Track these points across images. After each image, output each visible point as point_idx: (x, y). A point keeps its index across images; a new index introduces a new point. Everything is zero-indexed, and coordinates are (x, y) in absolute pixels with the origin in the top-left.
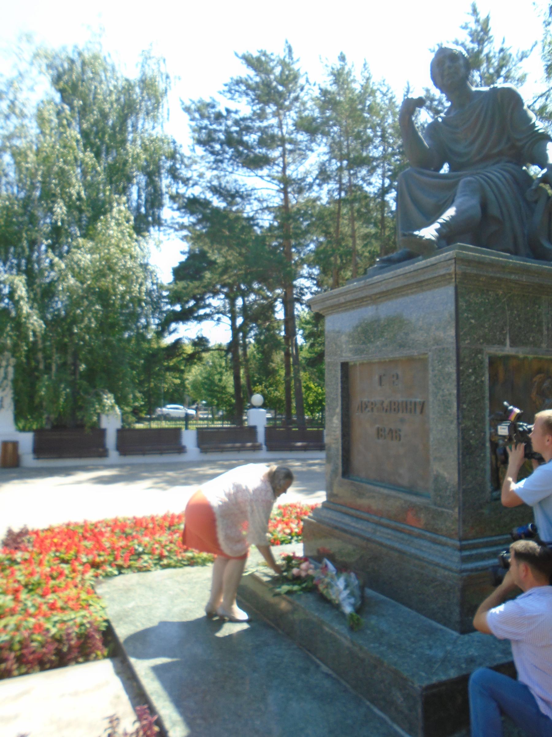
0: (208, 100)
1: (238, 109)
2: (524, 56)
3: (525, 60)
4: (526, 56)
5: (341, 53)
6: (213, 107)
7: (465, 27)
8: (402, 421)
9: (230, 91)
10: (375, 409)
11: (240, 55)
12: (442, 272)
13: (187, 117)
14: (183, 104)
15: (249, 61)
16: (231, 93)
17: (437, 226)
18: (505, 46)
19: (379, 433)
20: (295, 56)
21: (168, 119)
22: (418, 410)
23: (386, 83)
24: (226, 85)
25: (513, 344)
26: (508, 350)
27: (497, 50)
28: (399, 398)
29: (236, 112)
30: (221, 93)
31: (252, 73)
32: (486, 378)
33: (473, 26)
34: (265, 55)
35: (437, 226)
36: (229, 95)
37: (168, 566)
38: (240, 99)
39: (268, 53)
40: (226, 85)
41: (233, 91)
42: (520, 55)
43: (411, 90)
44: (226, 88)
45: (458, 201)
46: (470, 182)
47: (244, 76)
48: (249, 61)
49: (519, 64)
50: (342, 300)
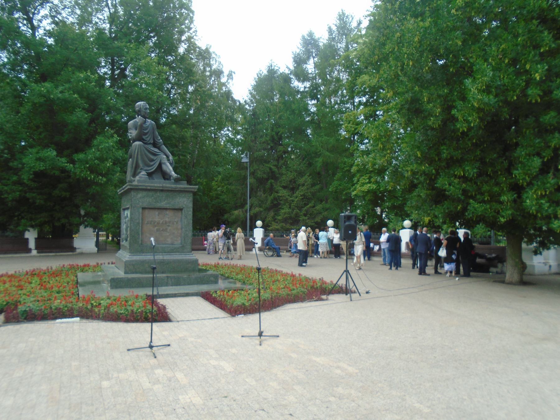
8: (169, 226)
10: (156, 223)
22: (175, 223)
28: (167, 219)
50: (149, 188)
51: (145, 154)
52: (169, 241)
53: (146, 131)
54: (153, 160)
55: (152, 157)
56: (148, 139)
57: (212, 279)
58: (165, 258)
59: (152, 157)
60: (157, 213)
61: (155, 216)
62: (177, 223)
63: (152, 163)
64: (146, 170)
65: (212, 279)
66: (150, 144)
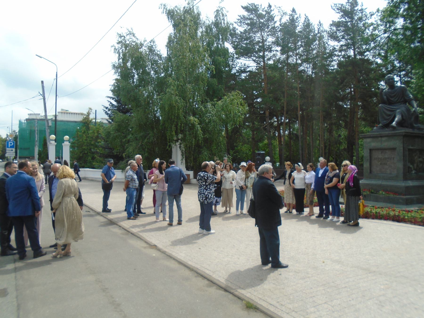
9: (241, 22)
19: (381, 164)
22: (392, 159)
28: (386, 156)
46: (399, 112)
51: (384, 112)
52: (388, 171)
53: (393, 95)
54: (390, 115)
55: (389, 113)
56: (396, 99)
57: (401, 201)
58: (383, 183)
59: (389, 113)
60: (380, 152)
61: (378, 155)
62: (393, 159)
63: (388, 118)
64: (383, 123)
65: (401, 201)
66: (399, 102)
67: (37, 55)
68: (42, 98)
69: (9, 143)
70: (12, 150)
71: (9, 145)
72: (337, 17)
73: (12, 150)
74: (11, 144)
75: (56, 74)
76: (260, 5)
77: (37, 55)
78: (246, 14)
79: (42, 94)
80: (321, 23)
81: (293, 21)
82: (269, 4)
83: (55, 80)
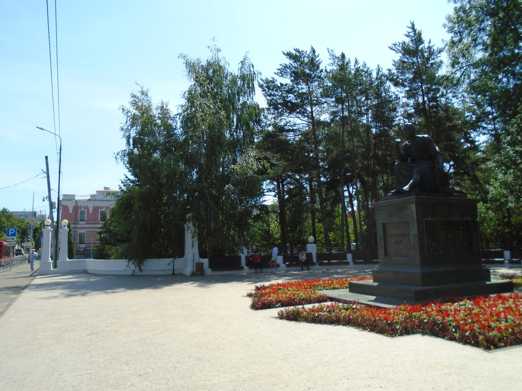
0: (271, 79)
1: (287, 83)
2: (440, 51)
3: (441, 53)
4: (442, 51)
5: (342, 53)
6: (274, 82)
7: (407, 36)
11: (286, 53)
12: (412, 200)
13: (261, 89)
14: (259, 84)
15: (289, 55)
16: (282, 74)
17: (408, 185)
18: (431, 45)
20: (316, 54)
21: (255, 94)
23: (366, 66)
24: (279, 70)
25: (431, 217)
26: (430, 219)
27: (426, 47)
29: (286, 85)
30: (276, 74)
31: (292, 62)
32: (425, 226)
33: (412, 34)
34: (299, 52)
35: (408, 185)
36: (280, 75)
37: (327, 289)
38: (286, 77)
39: (300, 50)
40: (279, 70)
41: (283, 73)
42: (438, 50)
43: (380, 70)
44: (279, 71)
45: (414, 176)
47: (288, 64)
48: (289, 55)
49: (439, 55)
50: (382, 205)
67: (37, 127)
68: (46, 175)
69: (10, 230)
70: (13, 239)
71: (10, 233)
72: (398, 56)
73: (13, 239)
74: (12, 231)
75: (60, 147)
76: (305, 51)
77: (37, 127)
78: (288, 61)
79: (45, 171)
80: (380, 67)
81: (343, 67)
82: (312, 48)
83: (59, 154)
